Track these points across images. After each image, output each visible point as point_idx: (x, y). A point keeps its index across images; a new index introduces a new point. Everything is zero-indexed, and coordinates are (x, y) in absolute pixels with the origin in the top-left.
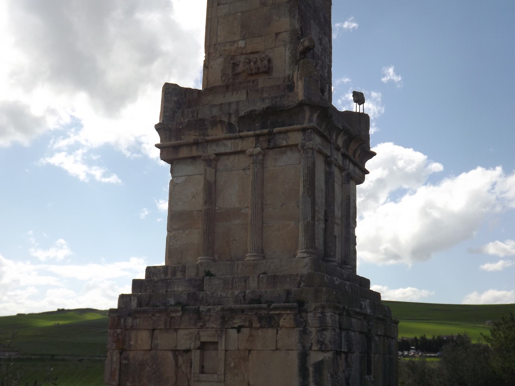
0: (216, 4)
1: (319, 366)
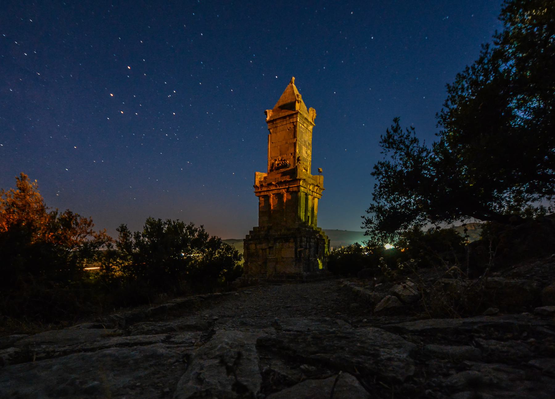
1: (300, 252)
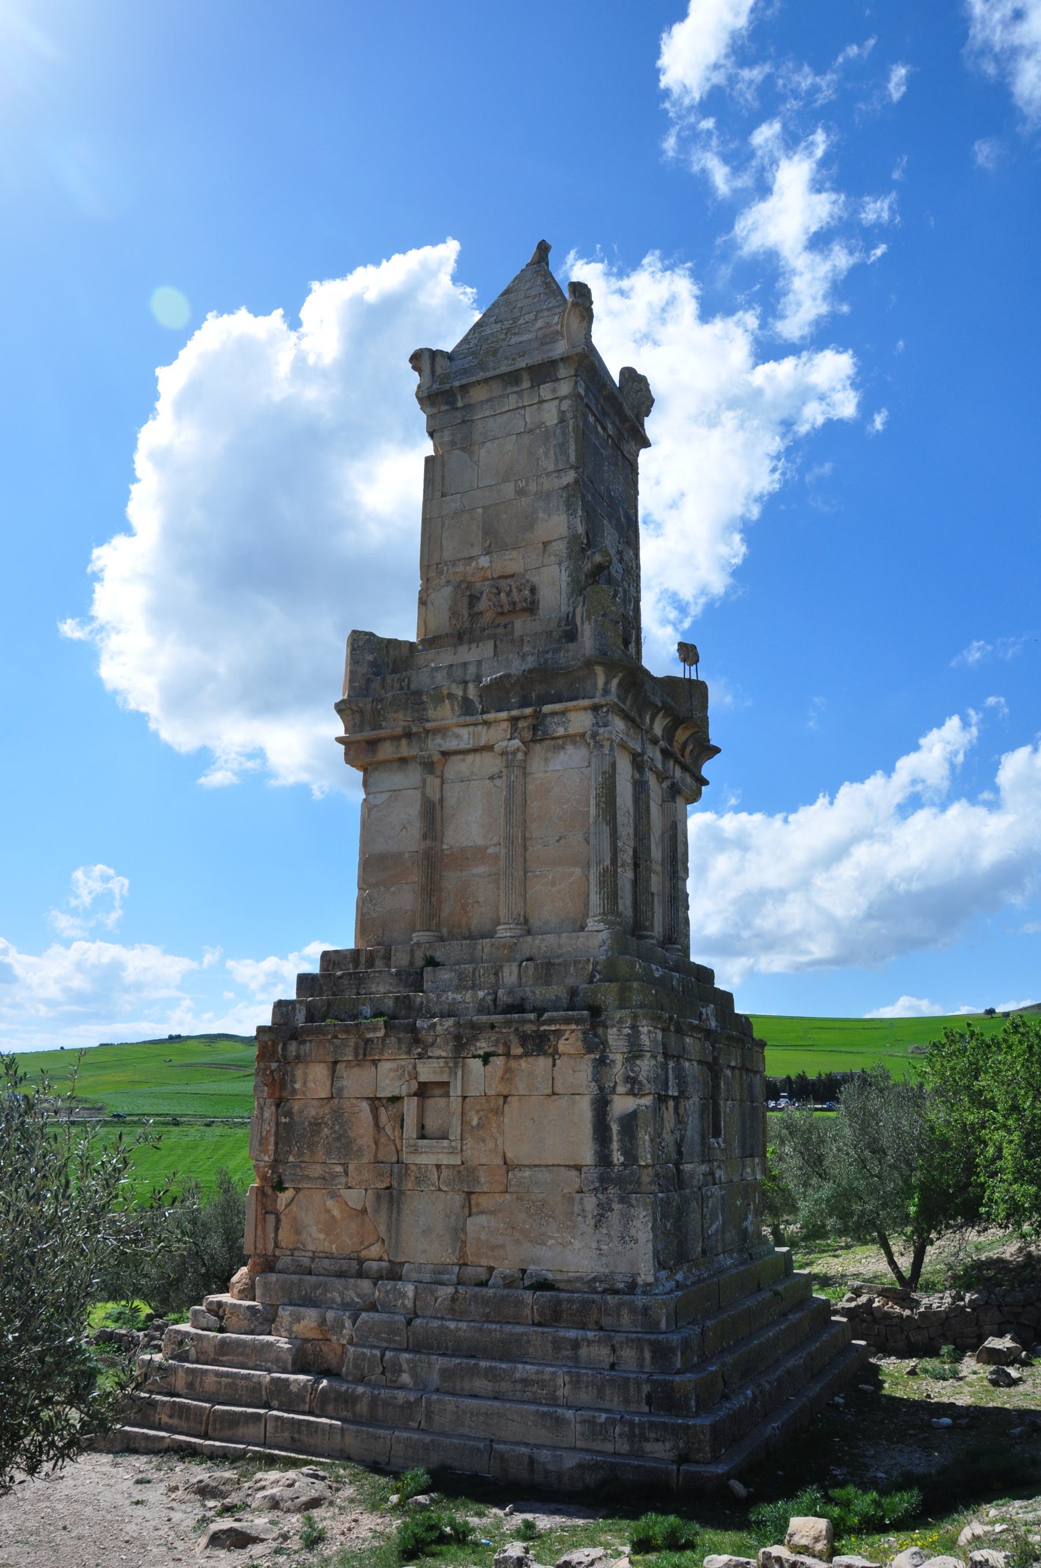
0: (438, 494)
1: (629, 1122)
